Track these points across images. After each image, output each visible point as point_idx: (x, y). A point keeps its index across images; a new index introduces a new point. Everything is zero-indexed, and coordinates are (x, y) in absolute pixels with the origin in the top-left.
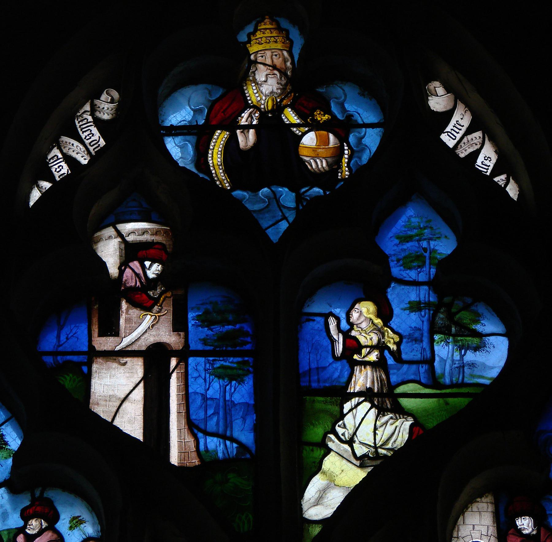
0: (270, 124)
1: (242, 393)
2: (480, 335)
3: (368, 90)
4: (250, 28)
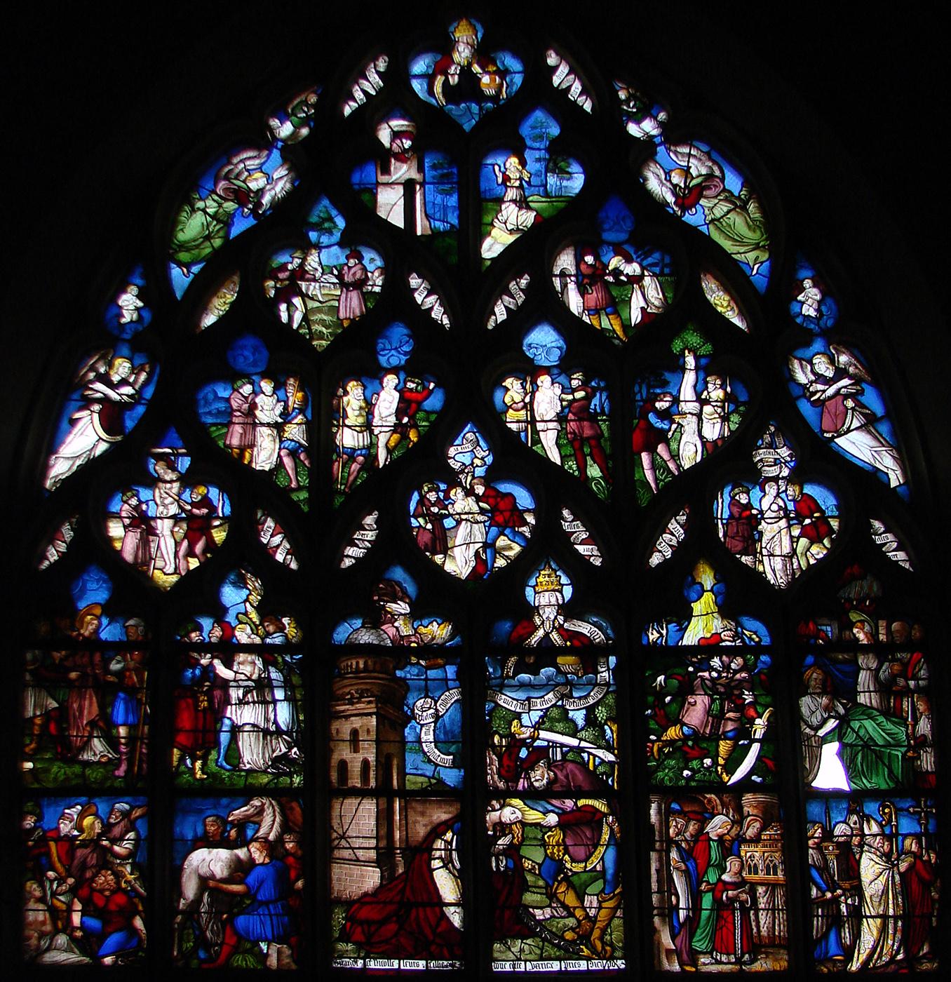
0: (466, 72)
1: (453, 201)
2: (570, 173)
3: (516, 55)
4: (456, 24)
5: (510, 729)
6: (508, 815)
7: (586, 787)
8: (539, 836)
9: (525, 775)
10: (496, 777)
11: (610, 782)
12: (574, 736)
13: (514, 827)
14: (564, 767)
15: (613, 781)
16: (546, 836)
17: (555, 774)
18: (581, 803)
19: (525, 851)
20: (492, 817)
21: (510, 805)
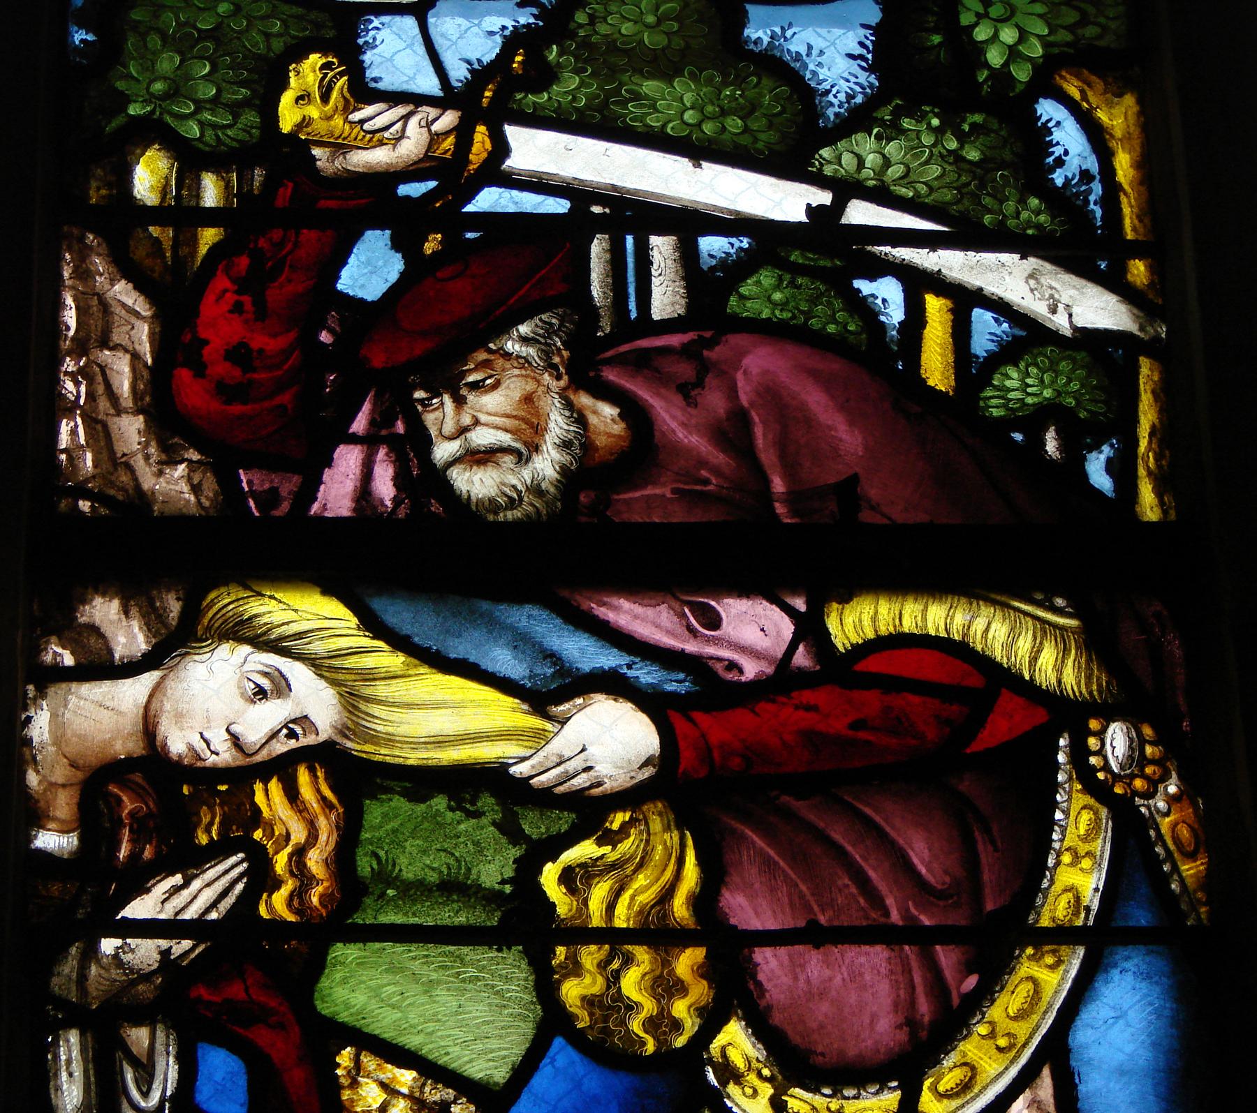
5: (271, 116)
6: (215, 703)
7: (894, 498)
8: (495, 870)
9: (380, 421)
10: (130, 430)
11: (1097, 472)
12: (787, 163)
13: (270, 798)
14: (704, 368)
15: (1122, 469)
16: (549, 876)
17: (633, 411)
18: (855, 622)
19: (359, 986)
20: (86, 718)
21: (242, 632)
